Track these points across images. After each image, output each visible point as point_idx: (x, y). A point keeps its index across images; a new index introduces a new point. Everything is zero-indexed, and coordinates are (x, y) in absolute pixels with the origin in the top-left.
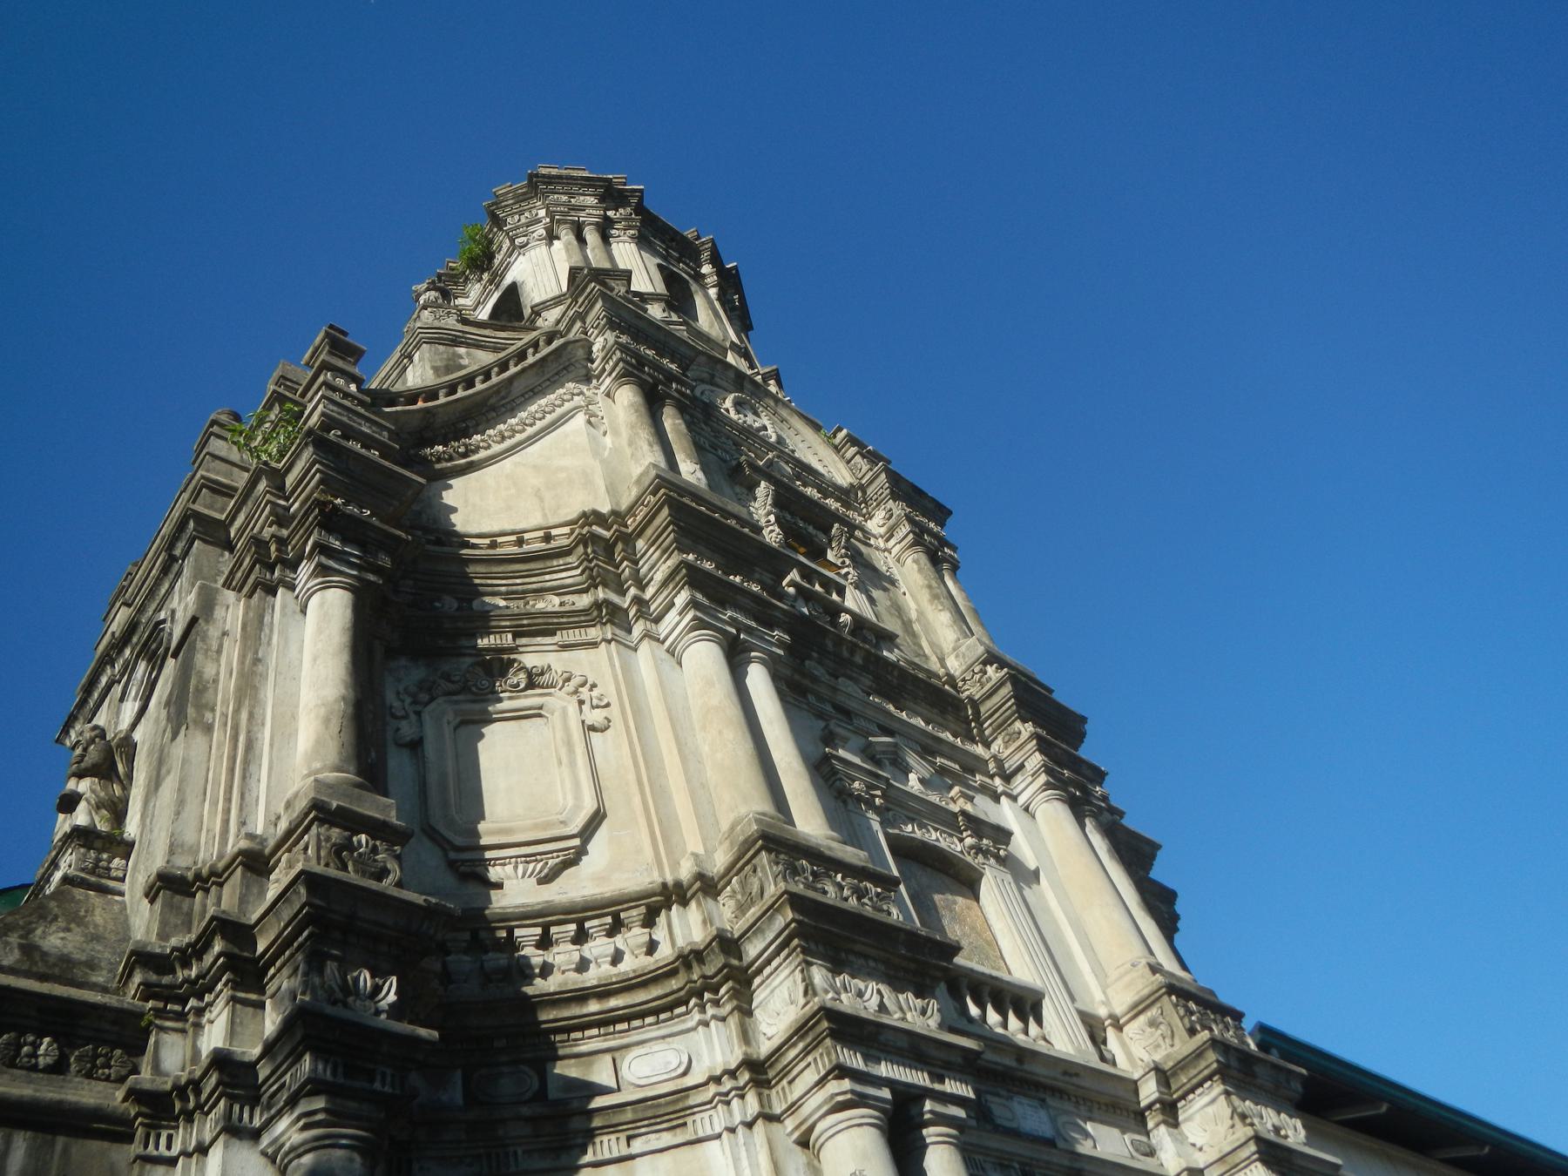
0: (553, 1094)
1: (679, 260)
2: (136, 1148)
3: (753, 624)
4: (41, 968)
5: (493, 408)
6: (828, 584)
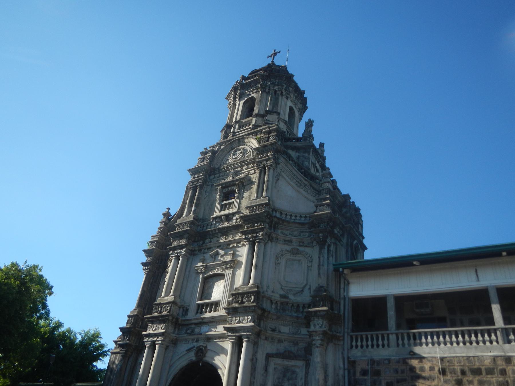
3: (179, 251)
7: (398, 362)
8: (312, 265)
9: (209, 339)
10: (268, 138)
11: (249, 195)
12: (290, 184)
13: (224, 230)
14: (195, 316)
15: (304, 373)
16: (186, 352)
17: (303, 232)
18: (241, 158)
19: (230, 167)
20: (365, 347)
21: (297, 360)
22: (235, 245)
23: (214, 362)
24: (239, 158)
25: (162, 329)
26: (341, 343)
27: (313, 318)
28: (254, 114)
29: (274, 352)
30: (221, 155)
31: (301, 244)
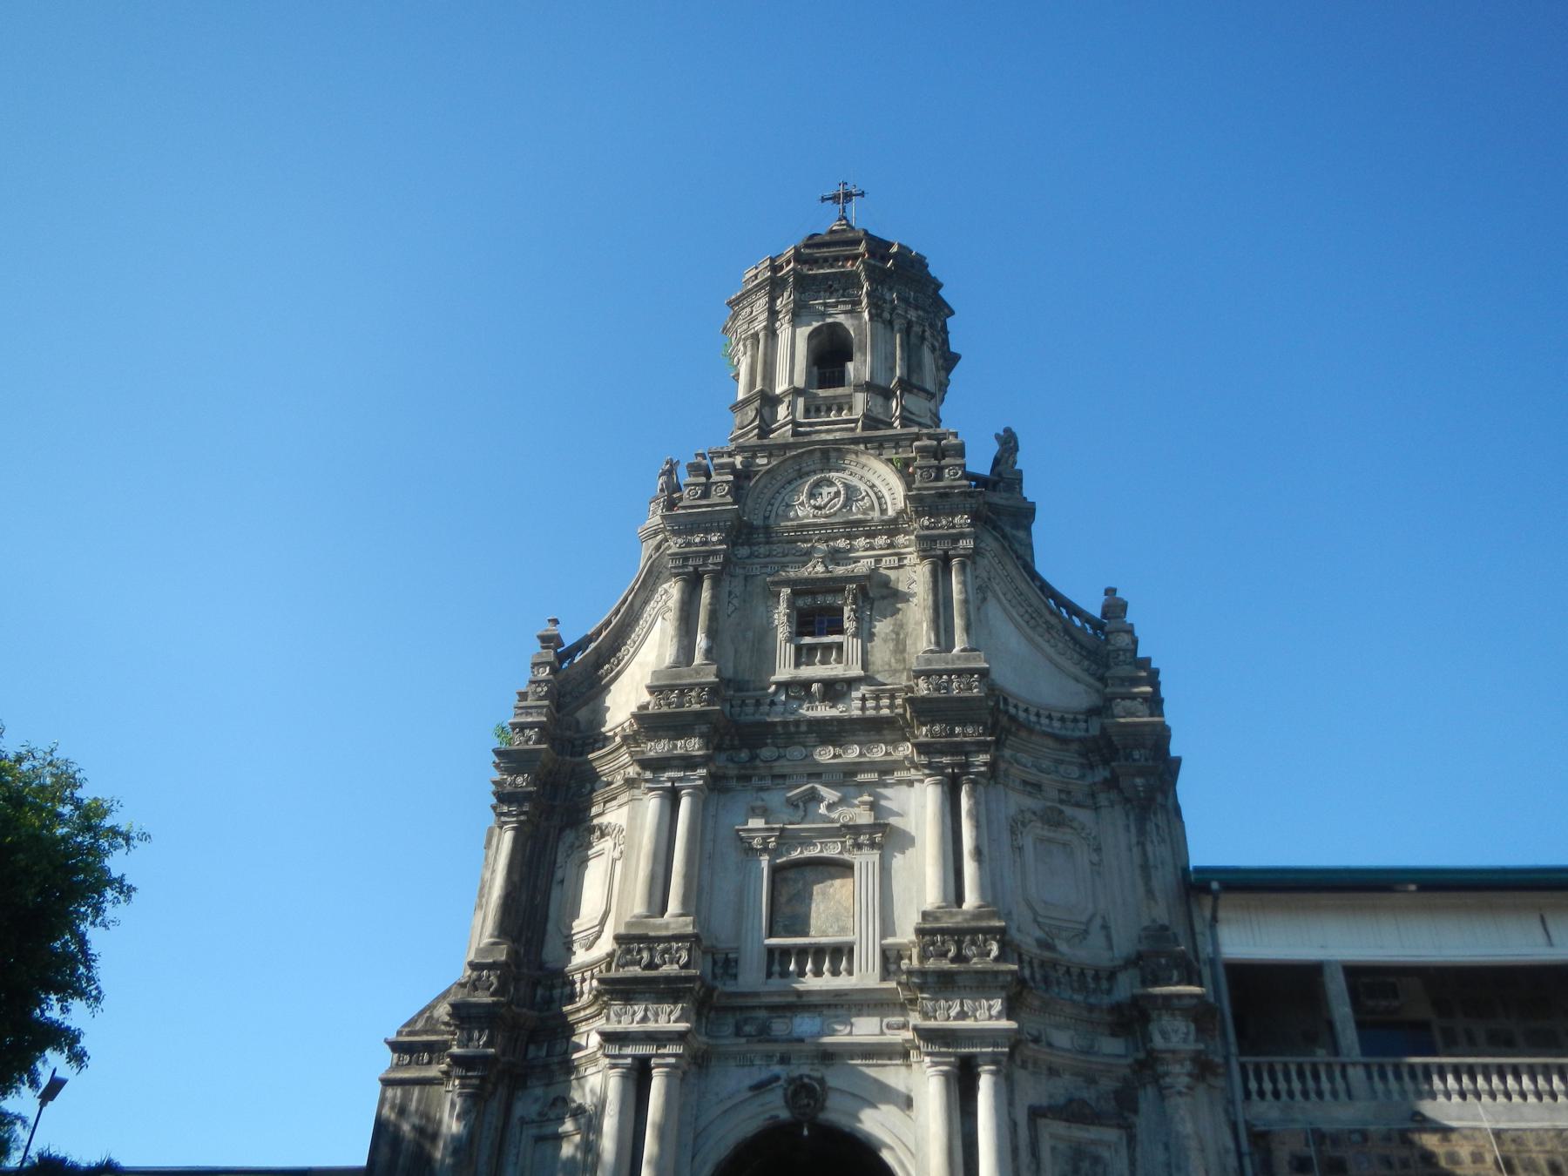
0: (570, 1050)
1: (835, 305)
2: (443, 1089)
3: (682, 774)
4: (428, 1027)
5: (629, 625)
6: (827, 648)
7: (1387, 1138)
8: (1101, 860)
9: (829, 1056)
10: (940, 469)
11: (893, 631)
12: (1012, 619)
13: (830, 728)
14: (766, 984)
15: (1126, 1161)
16: (750, 1094)
17: (1062, 762)
18: (840, 509)
19: (808, 531)
20: (1284, 1097)
21: (1101, 1125)
22: (873, 777)
23: (859, 1125)
24: (830, 509)
25: (672, 1018)
26: (1220, 1082)
27: (1156, 1012)
29: (1044, 1102)
30: (765, 487)
31: (1063, 796)
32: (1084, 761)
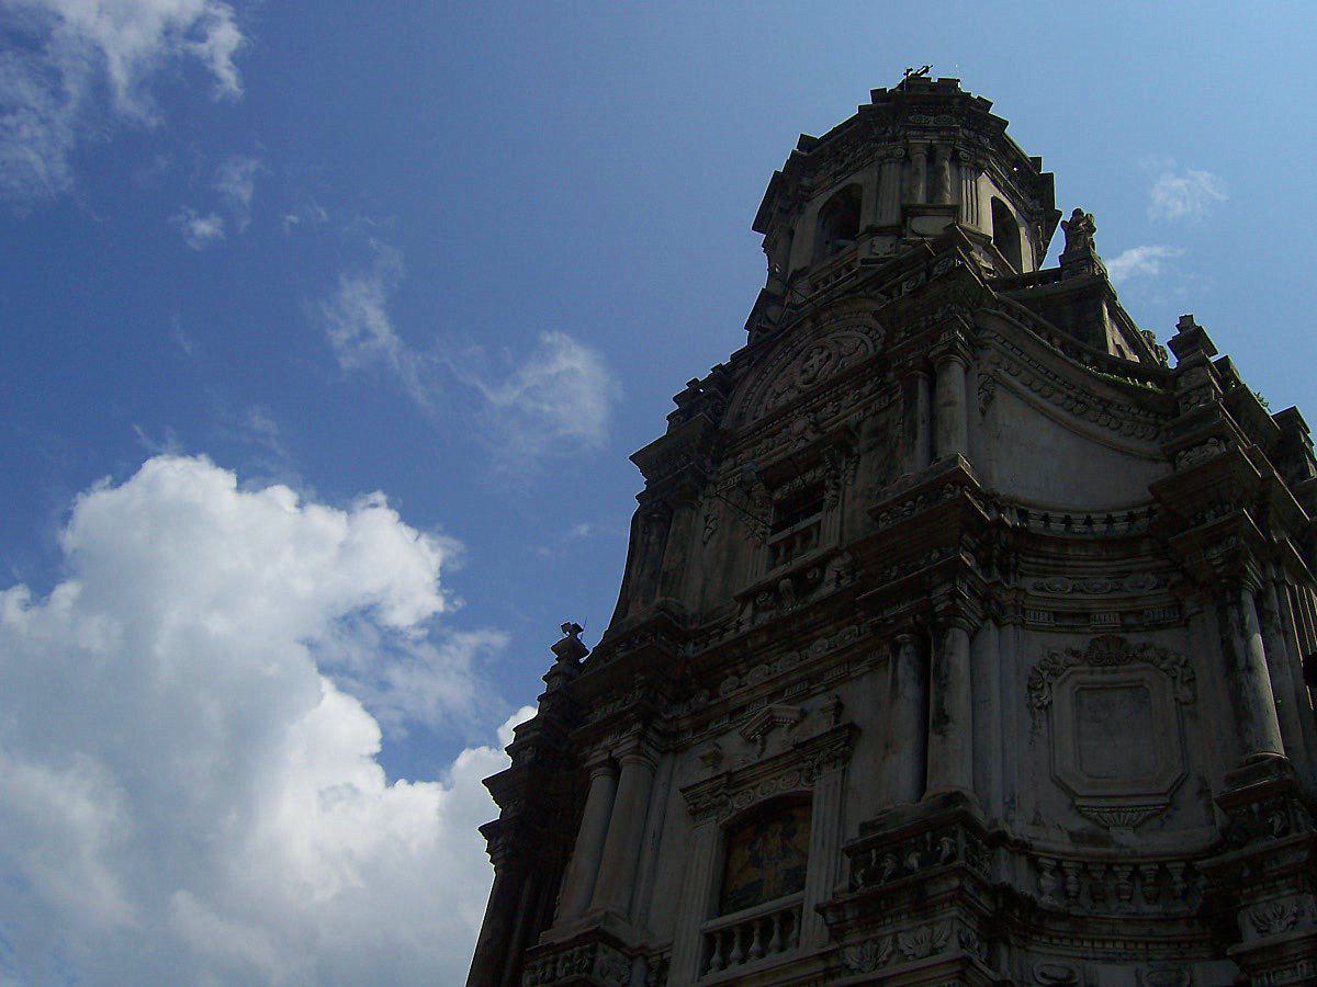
28: (862, 228)
31: (1130, 620)
32: (1159, 563)
